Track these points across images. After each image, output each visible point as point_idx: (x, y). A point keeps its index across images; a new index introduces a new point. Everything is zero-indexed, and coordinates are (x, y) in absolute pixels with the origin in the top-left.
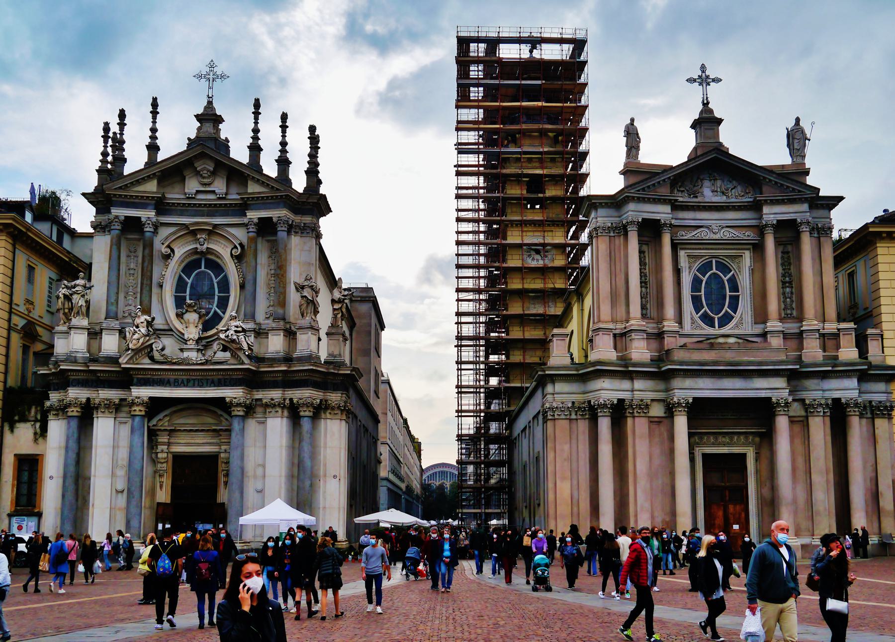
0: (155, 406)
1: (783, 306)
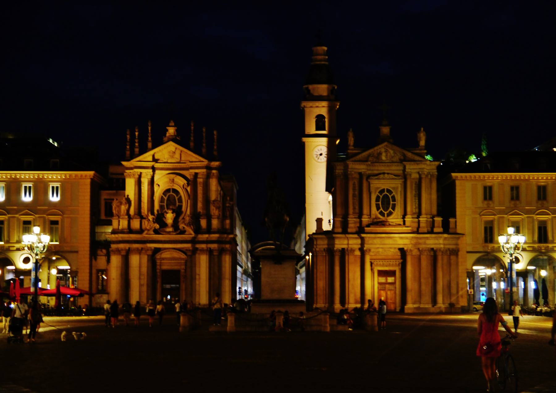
0: (157, 250)
1: (414, 207)
